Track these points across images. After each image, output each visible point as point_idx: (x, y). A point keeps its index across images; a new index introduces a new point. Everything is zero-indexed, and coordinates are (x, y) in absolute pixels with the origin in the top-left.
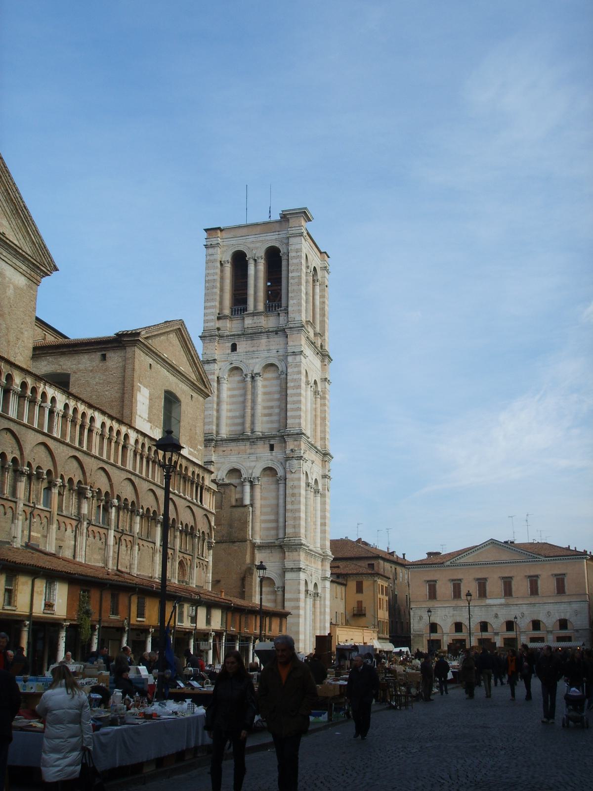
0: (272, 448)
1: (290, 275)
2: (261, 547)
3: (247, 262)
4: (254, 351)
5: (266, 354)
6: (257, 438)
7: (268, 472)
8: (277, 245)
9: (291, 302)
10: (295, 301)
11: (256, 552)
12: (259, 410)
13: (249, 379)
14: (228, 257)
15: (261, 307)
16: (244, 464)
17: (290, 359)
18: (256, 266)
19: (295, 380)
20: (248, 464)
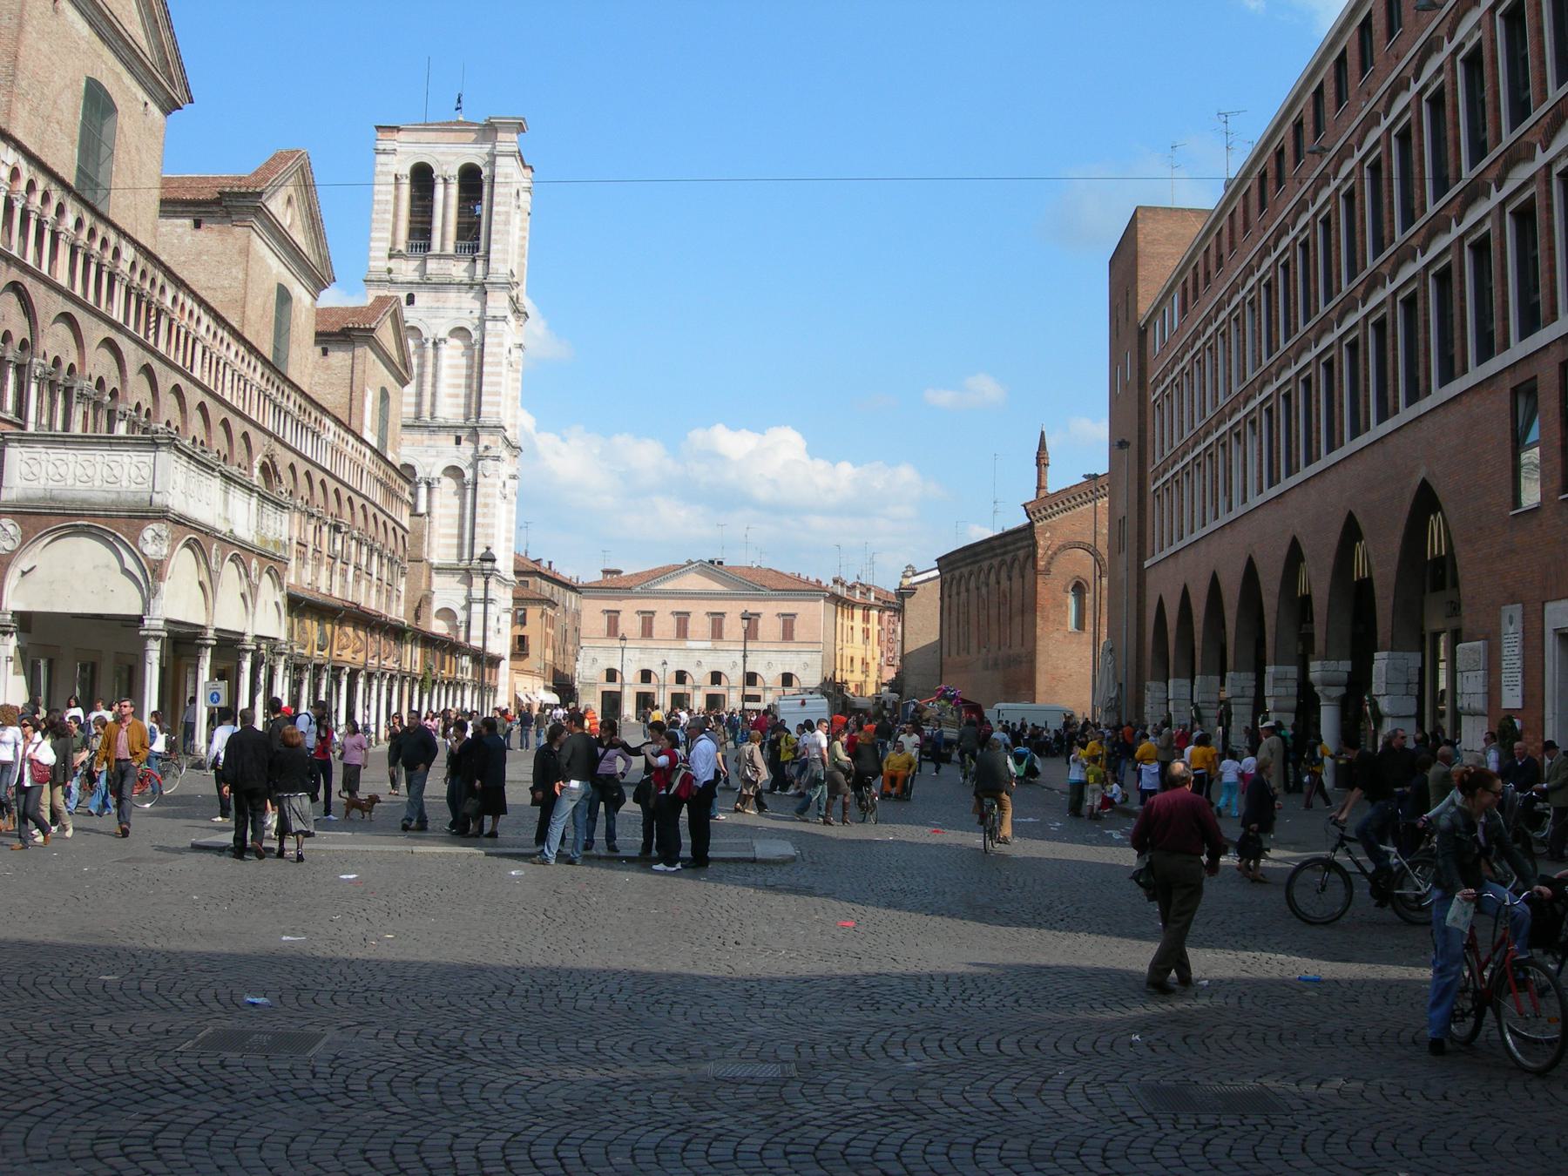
0: (458, 441)
1: (495, 209)
2: (440, 570)
3: (433, 180)
4: (438, 308)
5: (453, 314)
6: (439, 427)
7: (452, 472)
8: (479, 162)
9: (494, 247)
10: (499, 246)
11: (433, 575)
12: (443, 389)
13: (430, 345)
14: (406, 170)
15: (450, 249)
16: (420, 459)
17: (489, 325)
18: (446, 188)
19: (494, 355)
20: (424, 460)
